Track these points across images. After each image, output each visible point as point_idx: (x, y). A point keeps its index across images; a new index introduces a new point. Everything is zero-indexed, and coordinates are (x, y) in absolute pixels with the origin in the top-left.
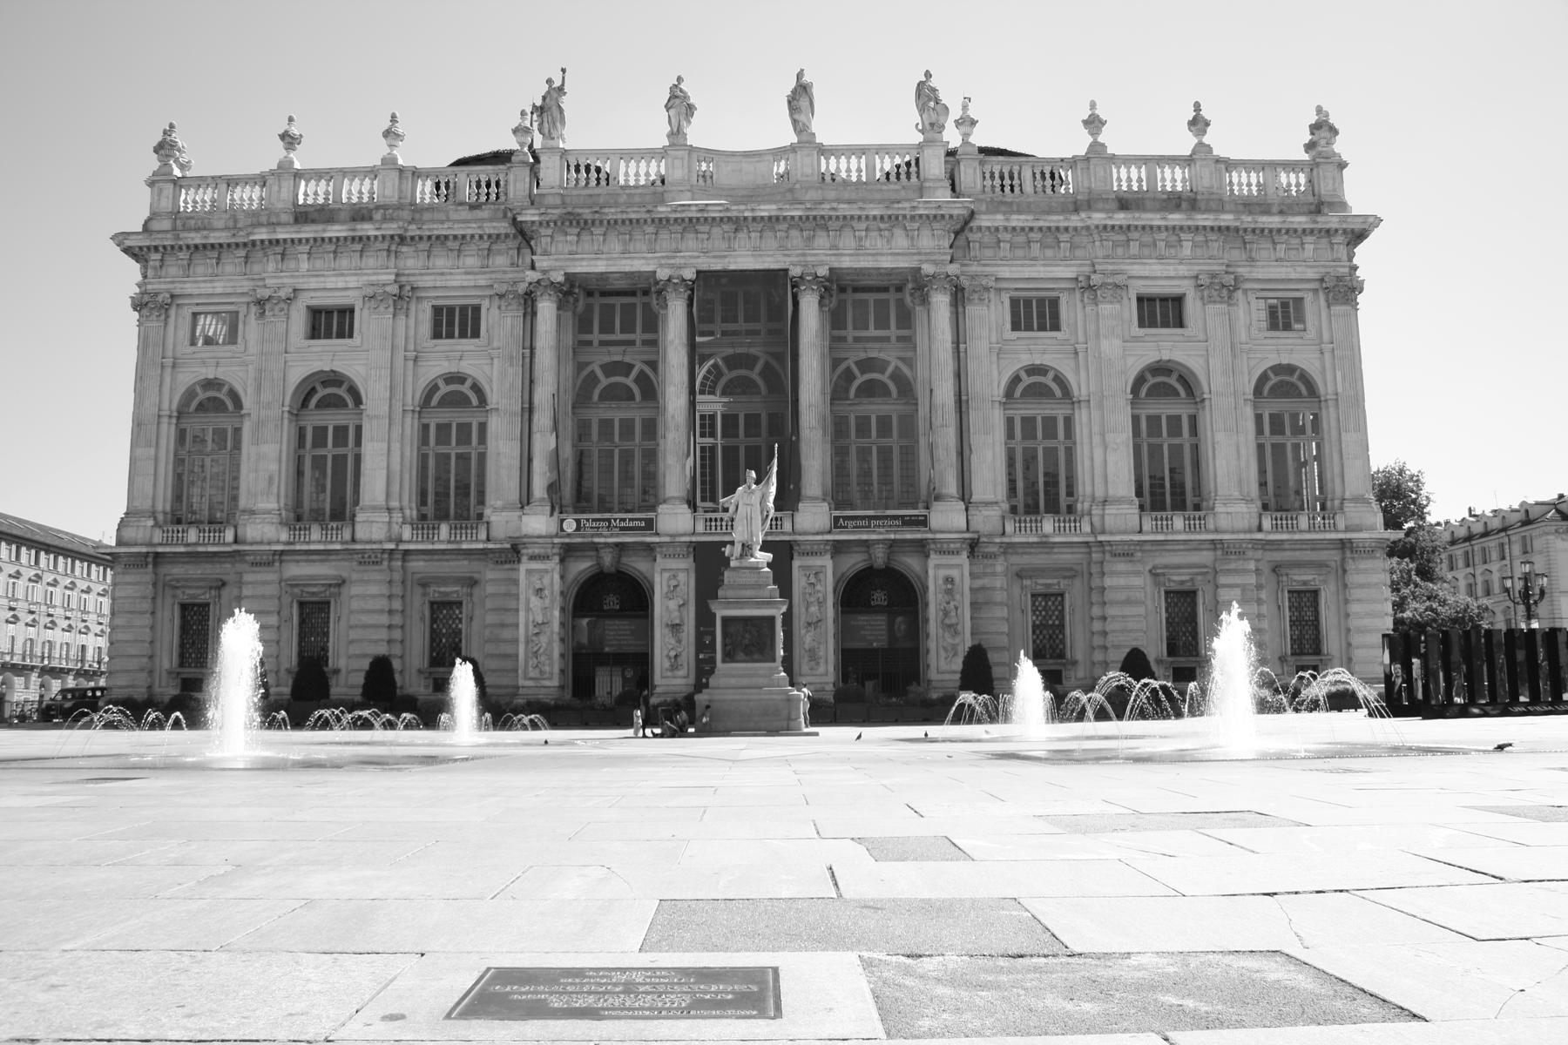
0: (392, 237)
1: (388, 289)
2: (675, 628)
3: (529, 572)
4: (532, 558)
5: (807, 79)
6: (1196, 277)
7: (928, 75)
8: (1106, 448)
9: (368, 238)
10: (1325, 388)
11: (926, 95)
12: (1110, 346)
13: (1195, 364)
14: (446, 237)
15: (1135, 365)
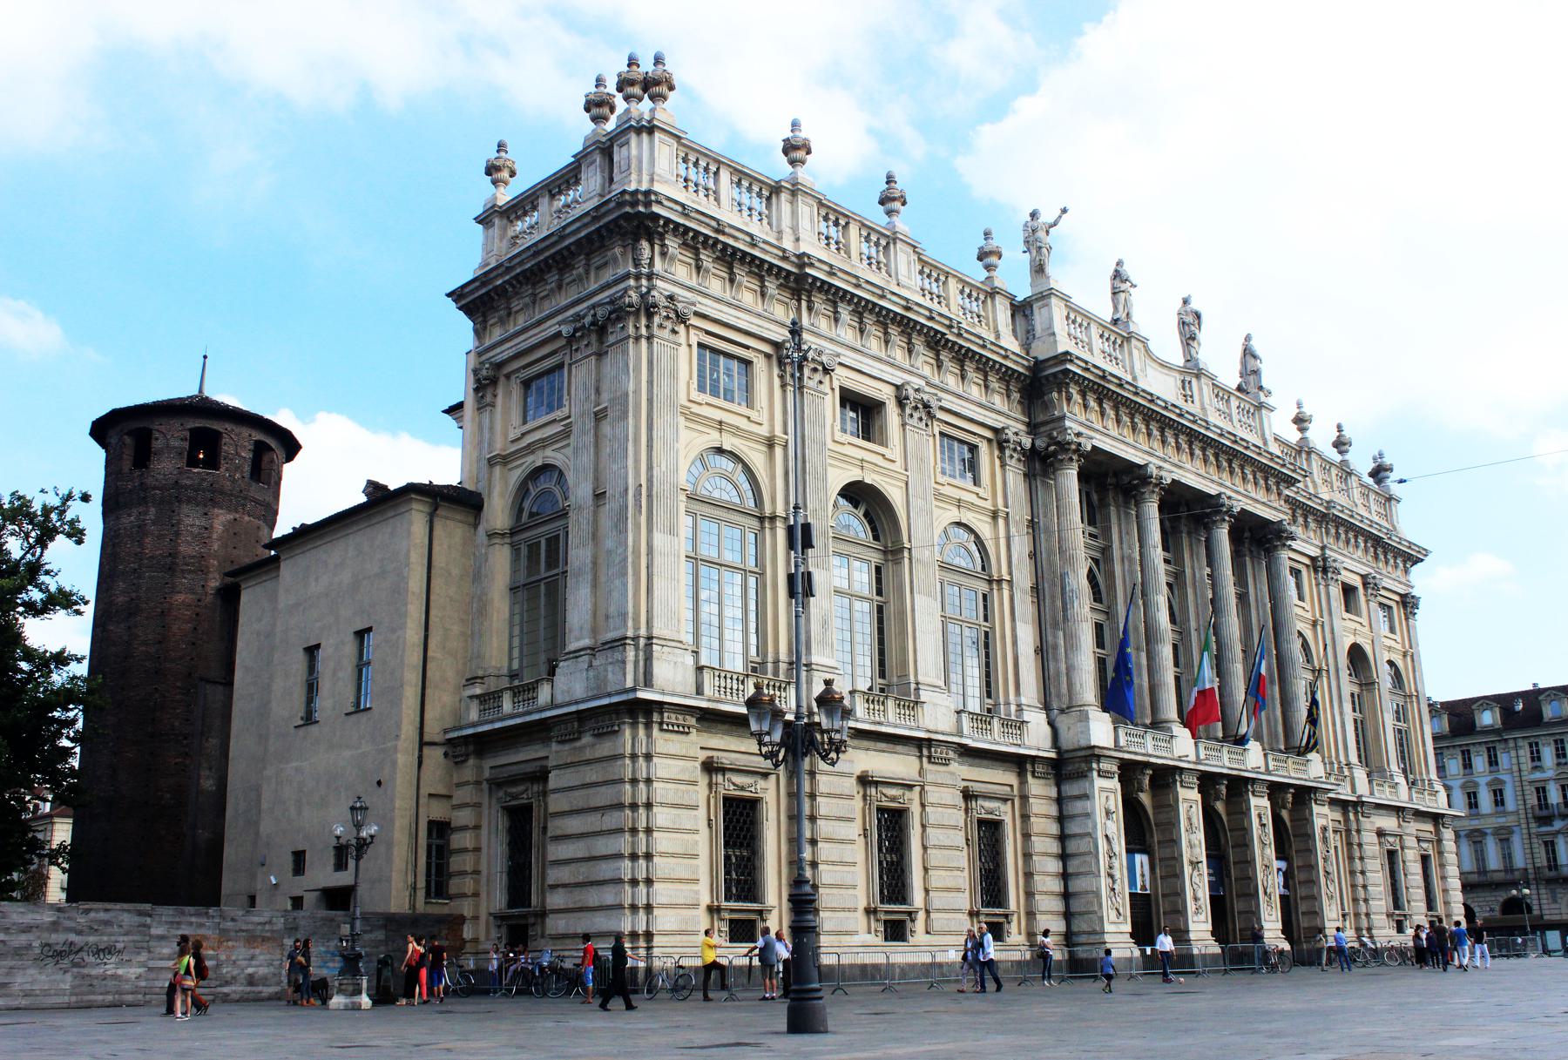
0: (937, 332)
1: (926, 397)
2: (1195, 864)
3: (1102, 790)
4: (1103, 774)
5: (1194, 305)
6: (1364, 577)
7: (1248, 338)
8: (1341, 714)
9: (916, 322)
10: (1409, 686)
11: (1248, 353)
12: (1337, 623)
13: (1368, 649)
14: (975, 353)
15: (1347, 642)
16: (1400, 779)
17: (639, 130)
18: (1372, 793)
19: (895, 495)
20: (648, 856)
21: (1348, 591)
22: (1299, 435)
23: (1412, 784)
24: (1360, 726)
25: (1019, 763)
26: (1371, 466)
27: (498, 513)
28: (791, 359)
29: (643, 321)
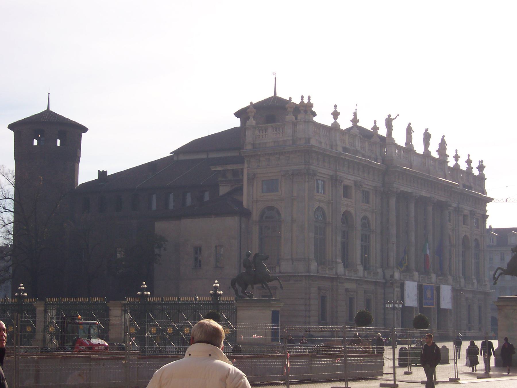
6: (471, 211)
7: (444, 136)
16: (475, 281)
17: (305, 122)
18: (465, 287)
19: (353, 212)
20: (309, 311)
21: (464, 216)
22: (455, 162)
23: (478, 281)
24: (464, 262)
25: (375, 283)
26: (477, 165)
27: (255, 216)
28: (335, 180)
29: (307, 177)
